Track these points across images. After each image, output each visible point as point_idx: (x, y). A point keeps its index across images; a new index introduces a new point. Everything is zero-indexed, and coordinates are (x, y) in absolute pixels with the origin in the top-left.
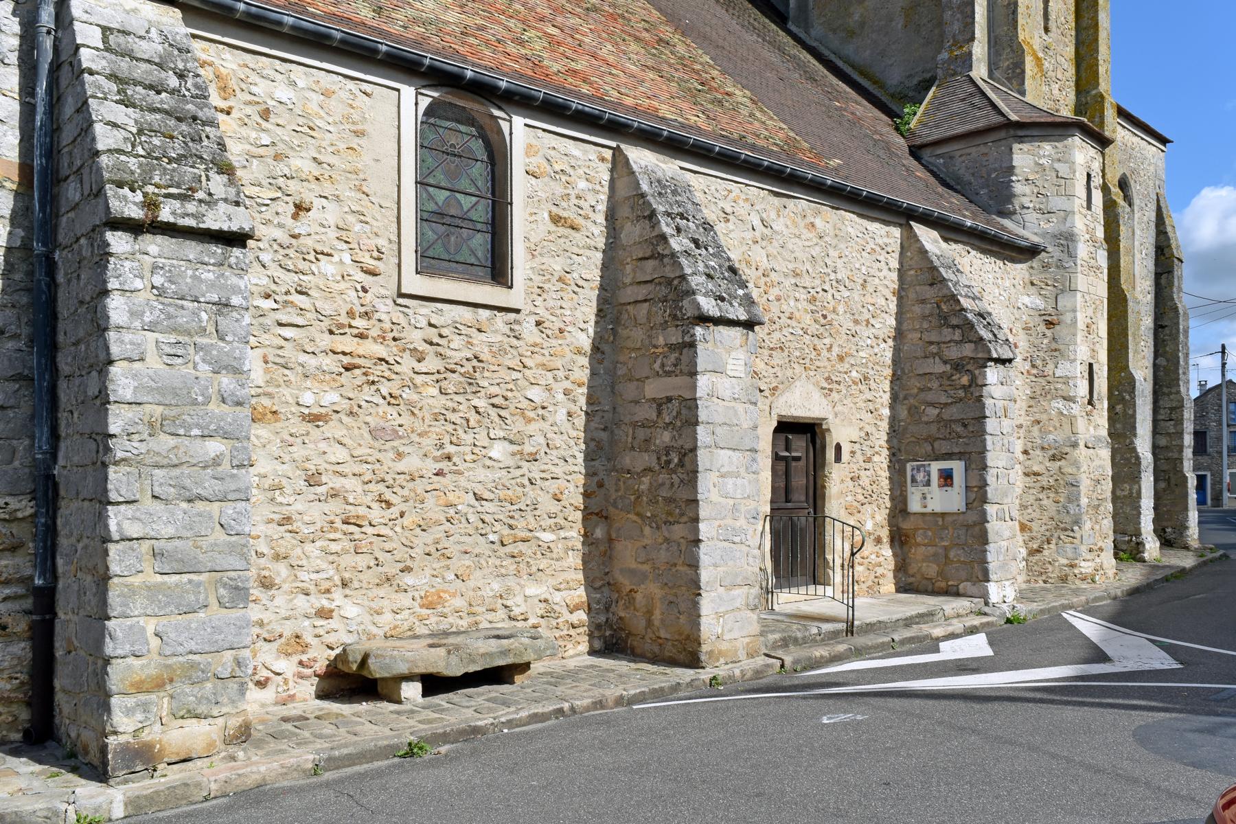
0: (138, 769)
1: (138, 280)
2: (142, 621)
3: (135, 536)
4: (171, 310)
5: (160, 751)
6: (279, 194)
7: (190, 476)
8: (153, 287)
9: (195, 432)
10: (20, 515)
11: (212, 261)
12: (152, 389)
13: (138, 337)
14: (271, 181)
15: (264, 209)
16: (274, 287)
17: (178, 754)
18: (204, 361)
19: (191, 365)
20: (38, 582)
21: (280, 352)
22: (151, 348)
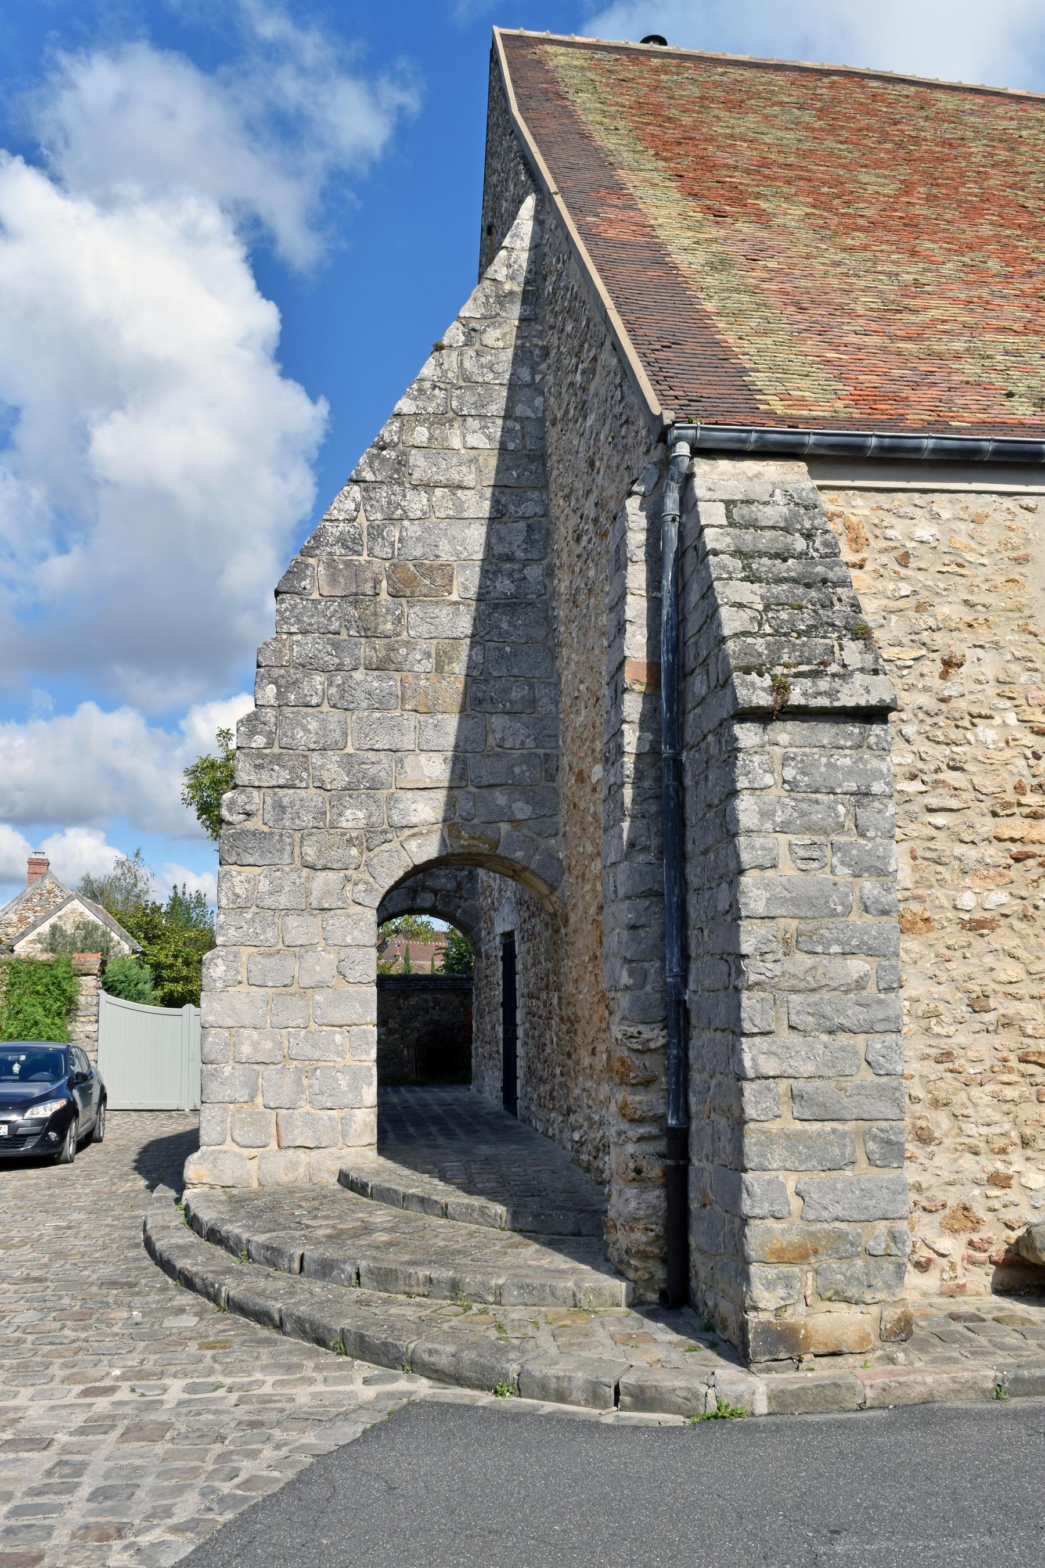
0: (782, 1356)
1: (768, 775)
2: (781, 1175)
3: (771, 1074)
4: (804, 806)
5: (805, 1337)
6: (924, 652)
7: (830, 1003)
8: (784, 782)
9: (835, 949)
10: (652, 1045)
11: (849, 744)
12: (786, 900)
13: (769, 841)
14: (913, 637)
15: (905, 672)
16: (920, 765)
17: (826, 1344)
18: (842, 863)
19: (828, 869)
20: (672, 1122)
21: (931, 845)
22: (783, 852)
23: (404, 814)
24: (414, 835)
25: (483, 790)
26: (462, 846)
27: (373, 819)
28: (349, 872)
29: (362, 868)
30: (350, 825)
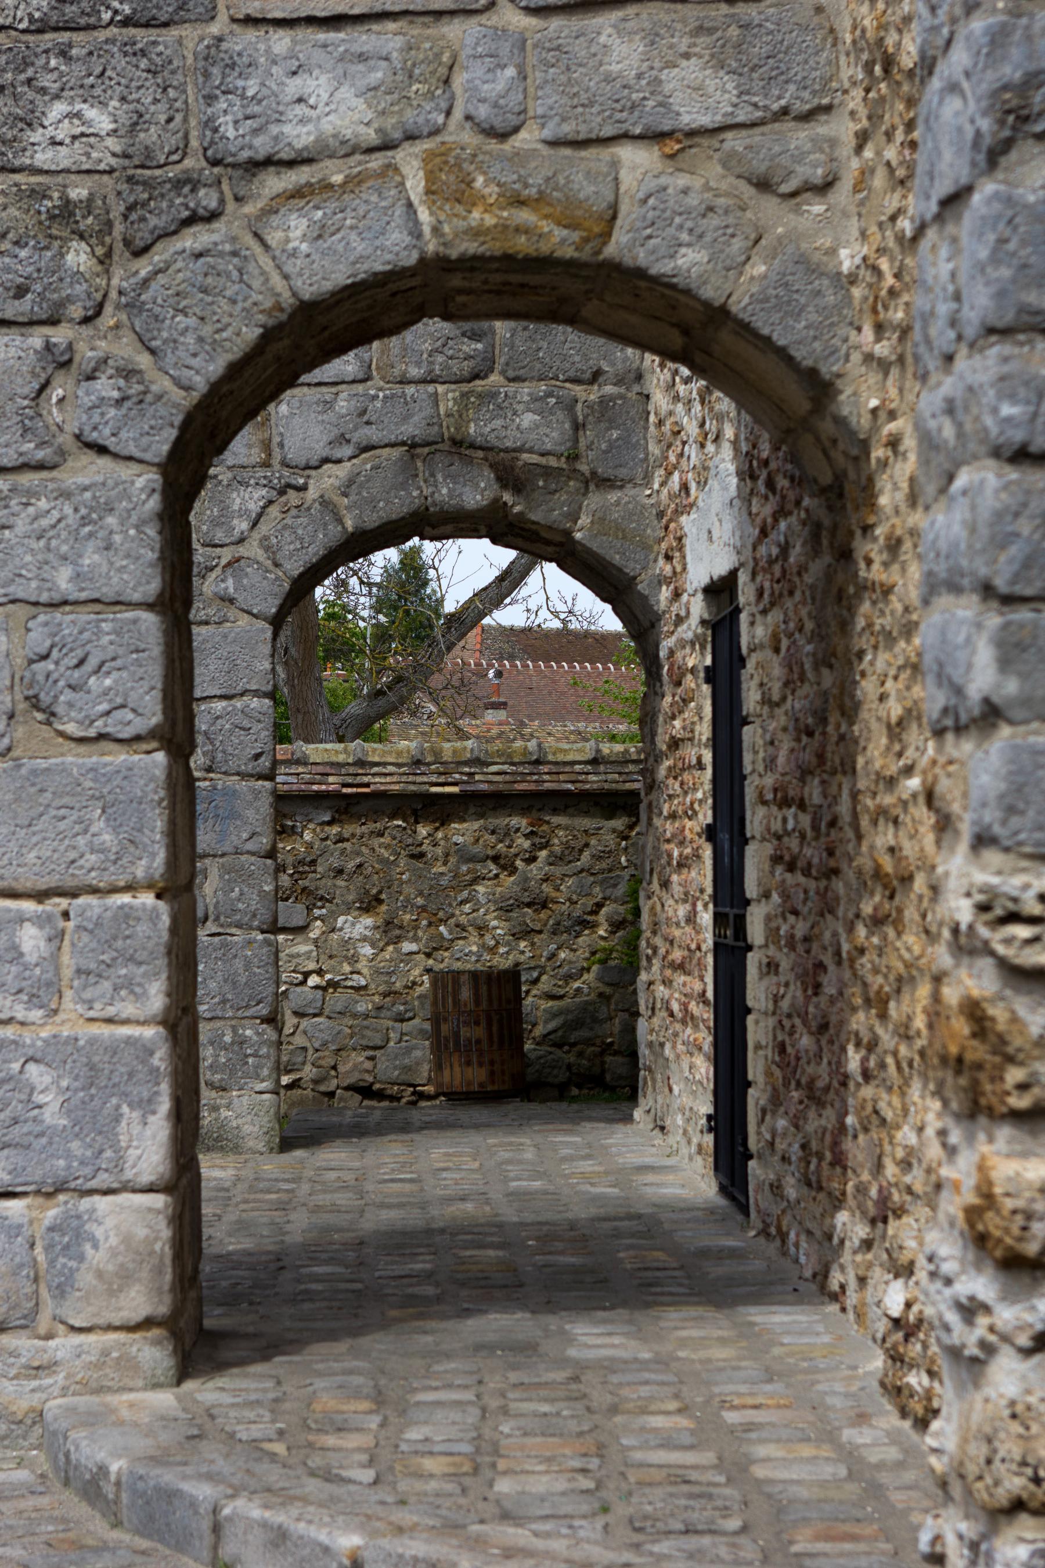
23: (262, 115)
24: (298, 193)
25: (556, 23)
26: (476, 233)
27: (150, 136)
28: (60, 335)
29: (108, 319)
30: (63, 157)
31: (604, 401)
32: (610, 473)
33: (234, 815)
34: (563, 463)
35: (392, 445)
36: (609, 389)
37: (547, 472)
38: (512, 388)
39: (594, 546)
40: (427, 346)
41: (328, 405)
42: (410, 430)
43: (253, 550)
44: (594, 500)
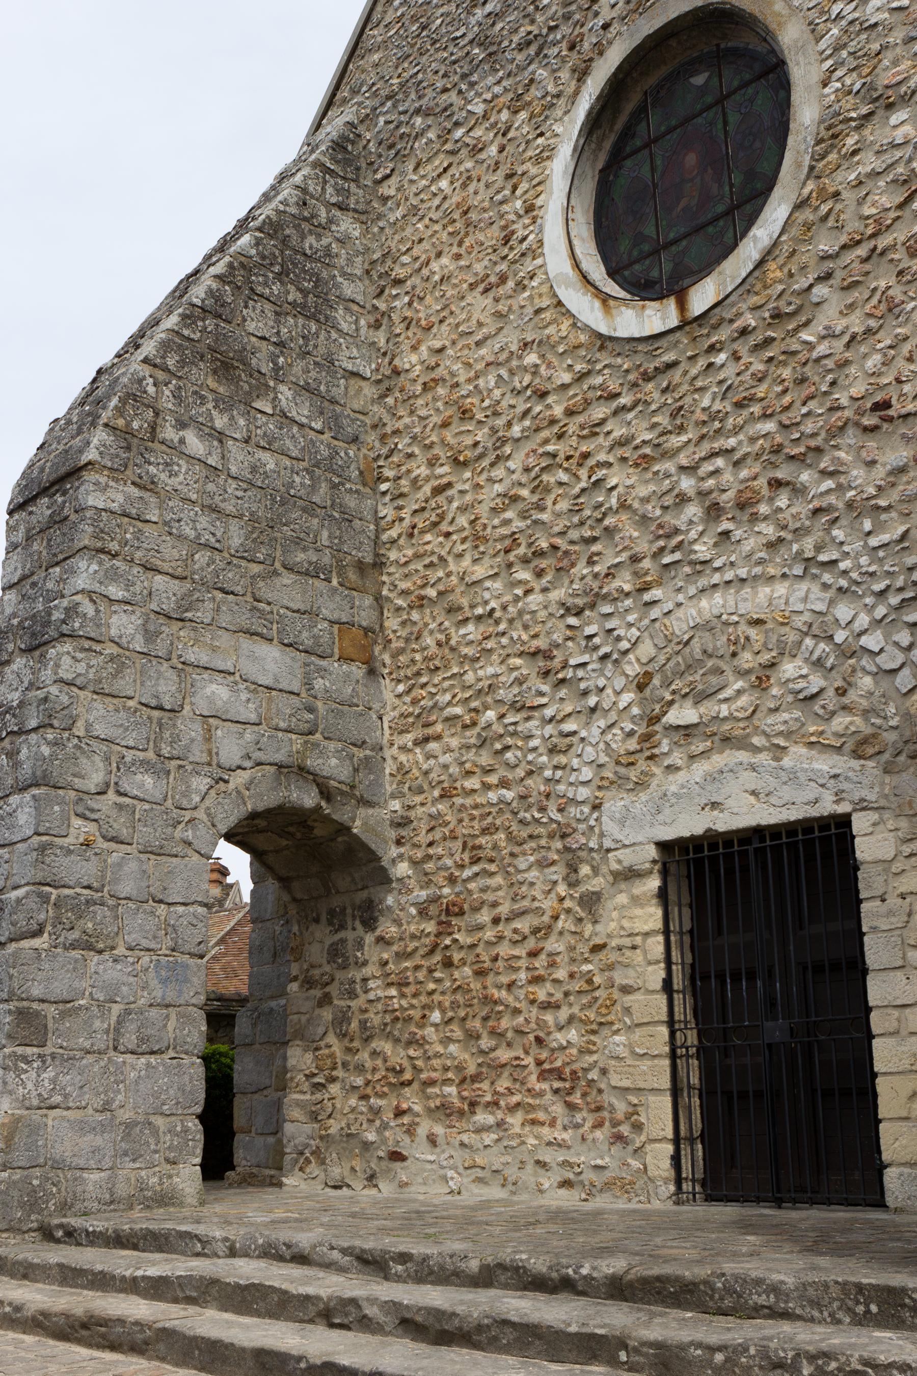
31: (367, 758)
32: (370, 798)
33: (186, 980)
34: (347, 789)
35: (271, 764)
36: (368, 752)
37: (342, 793)
38: (326, 743)
39: (363, 837)
40: (288, 711)
41: (241, 735)
42: (280, 757)
43: (201, 814)
44: (362, 812)
